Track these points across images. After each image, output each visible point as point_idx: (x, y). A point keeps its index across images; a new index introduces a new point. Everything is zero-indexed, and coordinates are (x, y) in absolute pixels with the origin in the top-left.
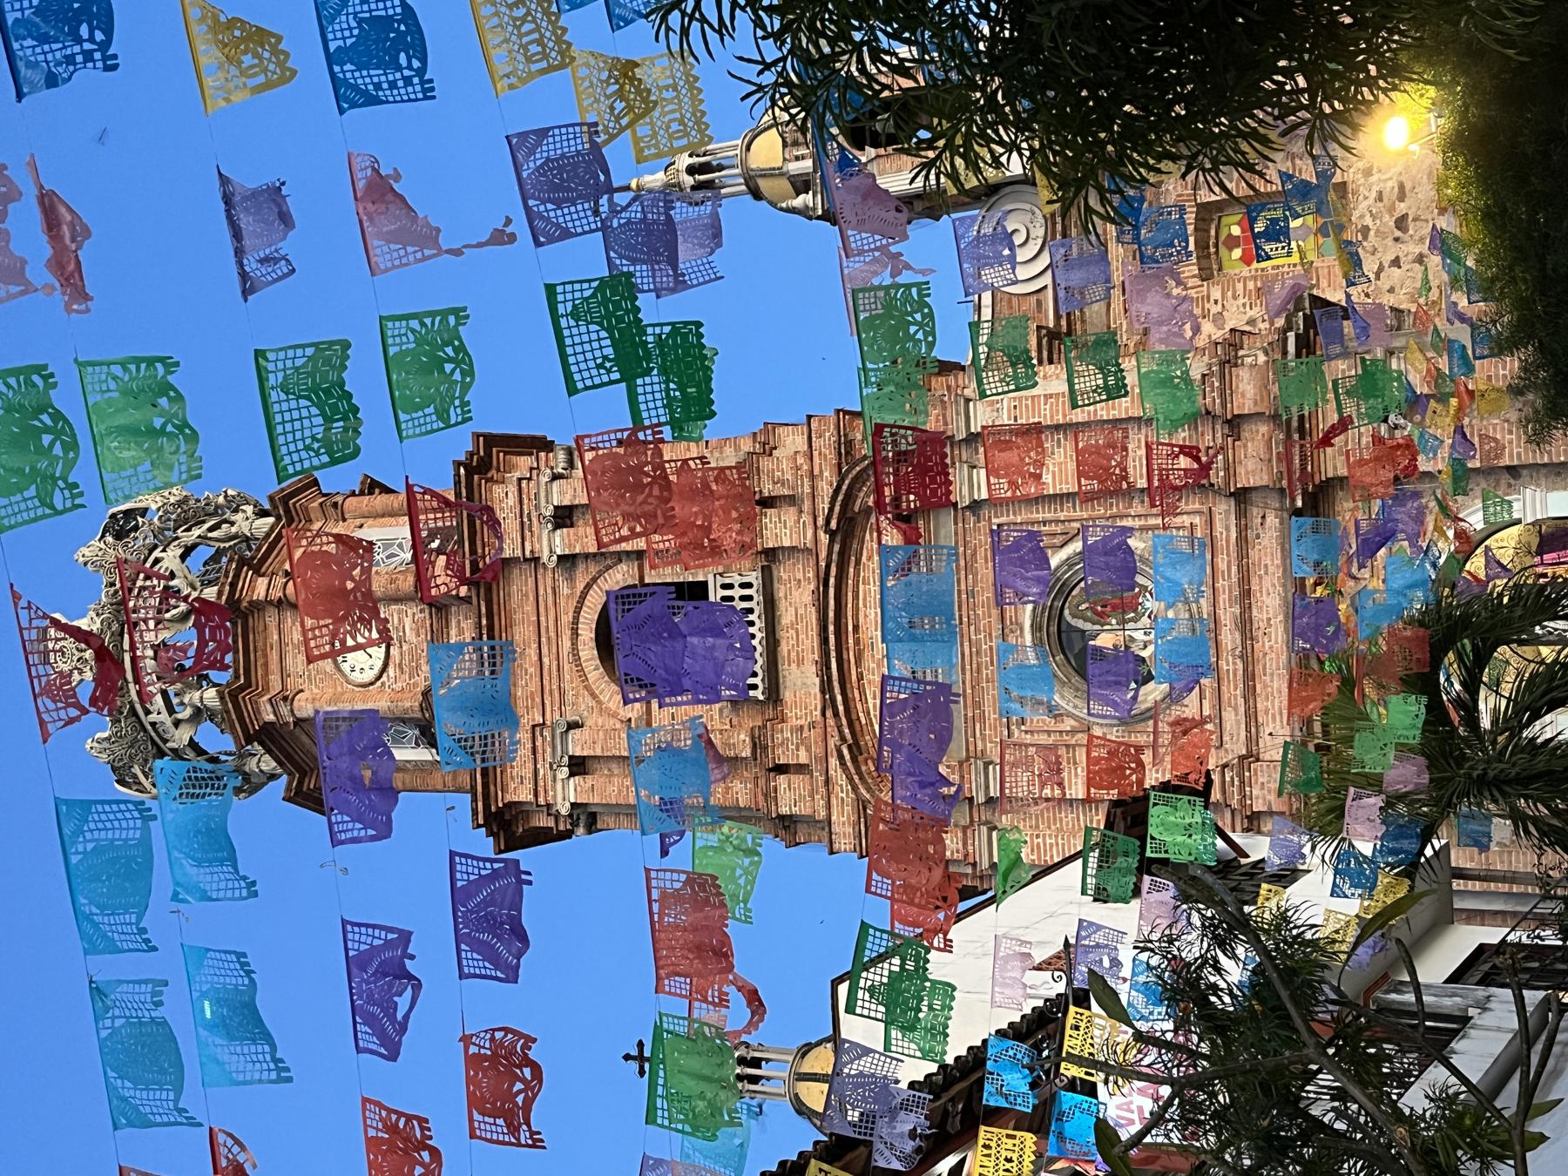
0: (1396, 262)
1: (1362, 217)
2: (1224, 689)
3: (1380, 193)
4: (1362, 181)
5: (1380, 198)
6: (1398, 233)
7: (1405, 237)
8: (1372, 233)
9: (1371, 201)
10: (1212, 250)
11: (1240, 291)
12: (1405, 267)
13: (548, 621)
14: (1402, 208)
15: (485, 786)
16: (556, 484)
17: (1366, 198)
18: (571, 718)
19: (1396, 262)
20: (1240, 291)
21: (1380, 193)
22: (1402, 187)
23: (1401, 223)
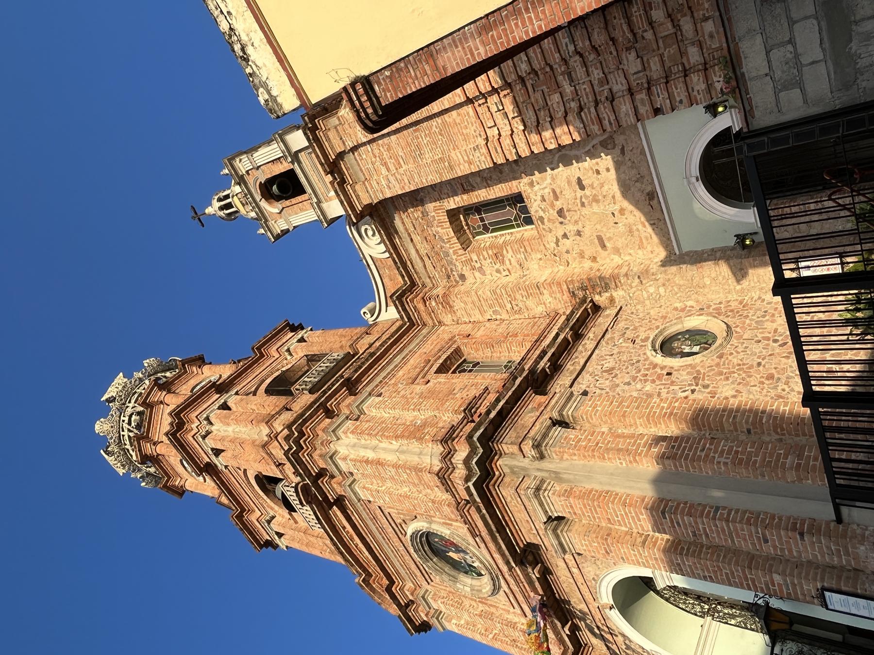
0: (565, 236)
1: (537, 211)
2: (517, 596)
3: (543, 196)
4: (529, 191)
5: (543, 199)
6: (561, 220)
7: (566, 221)
8: (546, 220)
9: (538, 202)
10: (466, 228)
11: (486, 256)
12: (571, 239)
13: (241, 481)
14: (558, 204)
15: (254, 538)
16: (207, 440)
17: (535, 201)
18: (272, 513)
19: (565, 236)
20: (486, 256)
21: (543, 196)
22: (554, 191)
23: (560, 212)
